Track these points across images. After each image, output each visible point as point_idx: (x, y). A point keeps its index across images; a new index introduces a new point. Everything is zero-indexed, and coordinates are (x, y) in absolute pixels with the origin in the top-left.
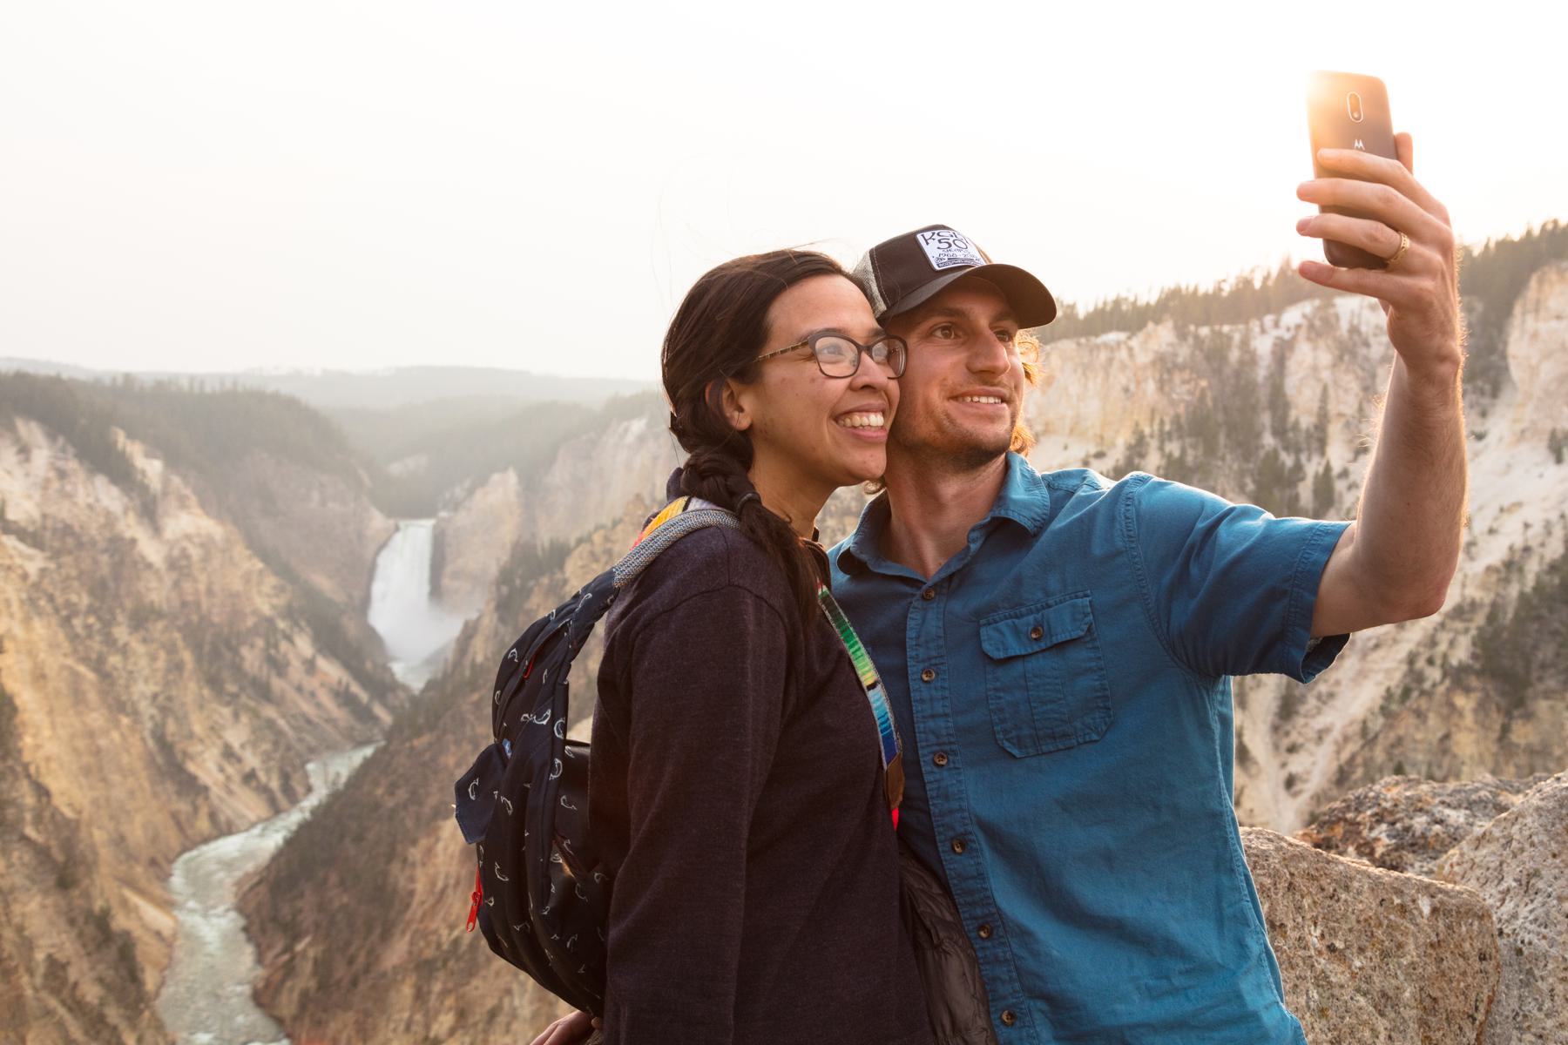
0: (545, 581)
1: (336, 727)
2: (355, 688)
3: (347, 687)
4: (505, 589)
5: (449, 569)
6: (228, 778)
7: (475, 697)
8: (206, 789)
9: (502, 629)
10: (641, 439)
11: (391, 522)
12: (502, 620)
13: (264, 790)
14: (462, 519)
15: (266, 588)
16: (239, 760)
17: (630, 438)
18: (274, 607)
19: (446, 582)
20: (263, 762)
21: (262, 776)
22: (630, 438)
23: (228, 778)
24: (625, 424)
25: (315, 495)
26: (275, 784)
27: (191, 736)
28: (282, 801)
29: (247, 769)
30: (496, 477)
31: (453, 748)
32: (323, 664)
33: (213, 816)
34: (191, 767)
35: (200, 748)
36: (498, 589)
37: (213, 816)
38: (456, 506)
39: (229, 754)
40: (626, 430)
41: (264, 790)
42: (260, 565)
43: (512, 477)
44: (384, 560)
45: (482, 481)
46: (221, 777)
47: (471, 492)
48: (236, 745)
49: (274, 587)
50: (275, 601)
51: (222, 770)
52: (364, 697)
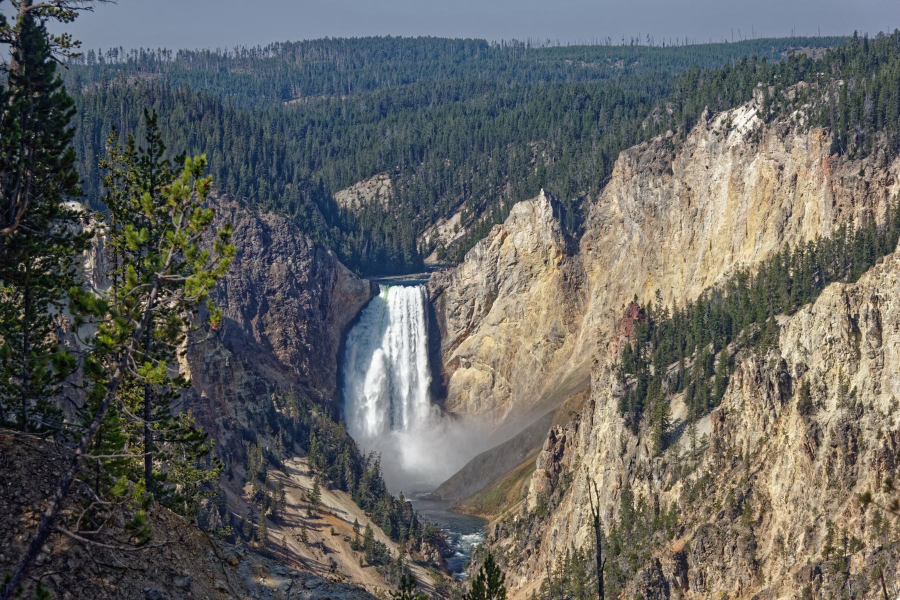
2: (379, 536)
3: (370, 533)
7: (677, 545)
9: (633, 440)
10: (755, 138)
11: (366, 282)
12: (633, 426)
14: (472, 273)
15: (236, 389)
17: (736, 139)
18: (250, 416)
22: (736, 139)
24: (724, 115)
25: (256, 245)
30: (520, 208)
32: (326, 499)
36: (622, 379)
38: (455, 257)
40: (729, 127)
42: (226, 354)
43: (542, 205)
49: (248, 384)
50: (250, 406)
52: (393, 550)
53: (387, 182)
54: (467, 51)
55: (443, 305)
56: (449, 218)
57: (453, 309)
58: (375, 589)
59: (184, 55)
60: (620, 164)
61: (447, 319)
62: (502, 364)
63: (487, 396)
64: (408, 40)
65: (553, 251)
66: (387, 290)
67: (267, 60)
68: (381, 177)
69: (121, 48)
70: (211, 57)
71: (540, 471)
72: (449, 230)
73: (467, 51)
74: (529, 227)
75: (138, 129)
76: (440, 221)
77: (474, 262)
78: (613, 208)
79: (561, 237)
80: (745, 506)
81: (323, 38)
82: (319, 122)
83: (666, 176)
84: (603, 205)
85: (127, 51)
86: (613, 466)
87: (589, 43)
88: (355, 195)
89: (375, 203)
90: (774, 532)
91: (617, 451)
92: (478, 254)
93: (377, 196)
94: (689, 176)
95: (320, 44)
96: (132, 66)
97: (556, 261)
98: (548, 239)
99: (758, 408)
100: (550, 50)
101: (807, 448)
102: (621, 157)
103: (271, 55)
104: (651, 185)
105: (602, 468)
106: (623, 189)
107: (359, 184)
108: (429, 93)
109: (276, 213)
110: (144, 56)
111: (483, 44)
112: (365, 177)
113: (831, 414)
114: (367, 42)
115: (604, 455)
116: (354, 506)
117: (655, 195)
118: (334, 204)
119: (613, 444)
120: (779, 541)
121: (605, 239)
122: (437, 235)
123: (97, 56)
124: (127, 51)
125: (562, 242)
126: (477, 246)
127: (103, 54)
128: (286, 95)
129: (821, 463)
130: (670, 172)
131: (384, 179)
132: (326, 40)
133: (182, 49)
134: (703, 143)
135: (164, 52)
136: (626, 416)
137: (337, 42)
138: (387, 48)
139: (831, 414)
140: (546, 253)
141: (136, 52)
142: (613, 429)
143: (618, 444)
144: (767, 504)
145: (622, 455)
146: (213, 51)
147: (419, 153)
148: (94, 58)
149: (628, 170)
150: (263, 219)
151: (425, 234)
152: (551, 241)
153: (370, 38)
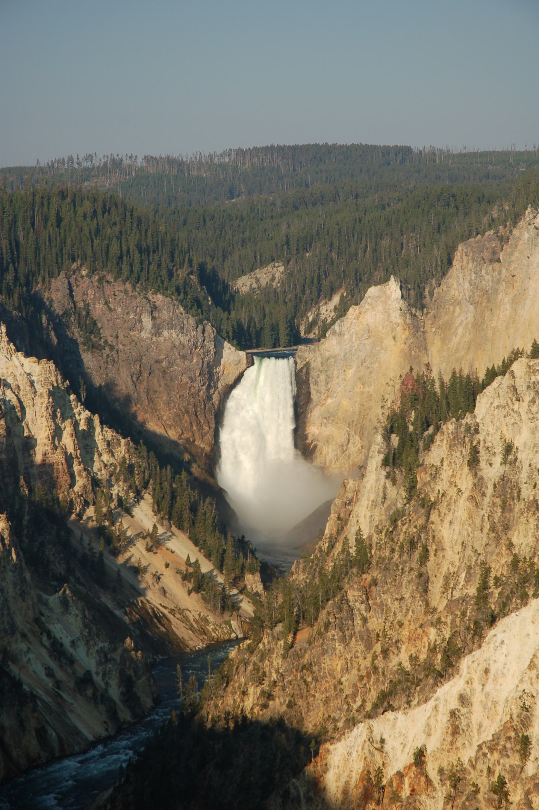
0: (450, 427)
1: (185, 620)
4: (395, 440)
5: (315, 415)
6: (58, 684)
8: (34, 697)
9: (392, 492)
13: (101, 698)
16: (72, 661)
19: (314, 430)
20: (99, 663)
21: (98, 679)
23: (58, 684)
26: (115, 692)
27: (13, 629)
28: (125, 715)
29: (81, 673)
30: (373, 291)
31: (339, 647)
33: (41, 734)
34: (14, 669)
35: (24, 646)
37: (41, 734)
39: (57, 650)
41: (101, 698)
43: (393, 288)
44: (230, 404)
45: (355, 297)
46: (49, 683)
47: (341, 311)
48: (66, 642)
51: (50, 673)
53: (282, 269)
54: (392, 156)
55: (308, 373)
56: (330, 300)
57: (315, 377)
58: (199, 615)
59: (148, 159)
60: (459, 254)
61: (311, 386)
62: (356, 425)
63: (344, 452)
64: (341, 147)
65: (399, 329)
66: (261, 361)
67: (222, 166)
68: (276, 264)
69: (96, 154)
70: (171, 161)
71: (333, 516)
72: (327, 309)
73: (392, 156)
74: (380, 308)
75: (49, 223)
76: (323, 302)
77: (334, 338)
78: (452, 292)
79: (408, 316)
80: (420, 547)
81: (269, 145)
82: (236, 219)
83: (496, 265)
84: (445, 289)
85: (100, 156)
86: (376, 512)
87: (482, 150)
88: (254, 280)
89: (269, 286)
90: (444, 570)
91: (380, 500)
92: (338, 331)
93: (273, 279)
94: (513, 265)
95: (269, 150)
96: (105, 170)
97: (404, 337)
98: (396, 317)
99: (453, 464)
100: (465, 155)
101: (472, 498)
102: (460, 248)
103: (227, 160)
104: (483, 272)
105: (369, 514)
106: (461, 276)
107: (257, 271)
108: (337, 193)
109: (163, 294)
110: (113, 160)
111: (407, 150)
112: (263, 264)
113: (493, 470)
114: (307, 148)
115: (370, 503)
116: (190, 544)
117: (487, 281)
118: (226, 287)
119: (378, 495)
120: (447, 578)
121: (446, 318)
122: (318, 315)
123: (75, 160)
124: (100, 156)
125: (408, 321)
126: (337, 324)
127: (80, 159)
128: (232, 194)
129: (485, 512)
130: (499, 261)
131: (279, 266)
132: (272, 147)
133: (147, 155)
134: (526, 236)
135: (130, 157)
136: (388, 469)
137: (281, 149)
138: (320, 154)
139: (493, 470)
140: (393, 329)
141: (107, 157)
142: (377, 480)
143: (381, 494)
144: (440, 548)
145: (383, 503)
146: (175, 156)
147: (306, 243)
148: (73, 163)
149: (465, 258)
150: (153, 300)
151: (310, 313)
152: (399, 320)
153: (310, 145)
